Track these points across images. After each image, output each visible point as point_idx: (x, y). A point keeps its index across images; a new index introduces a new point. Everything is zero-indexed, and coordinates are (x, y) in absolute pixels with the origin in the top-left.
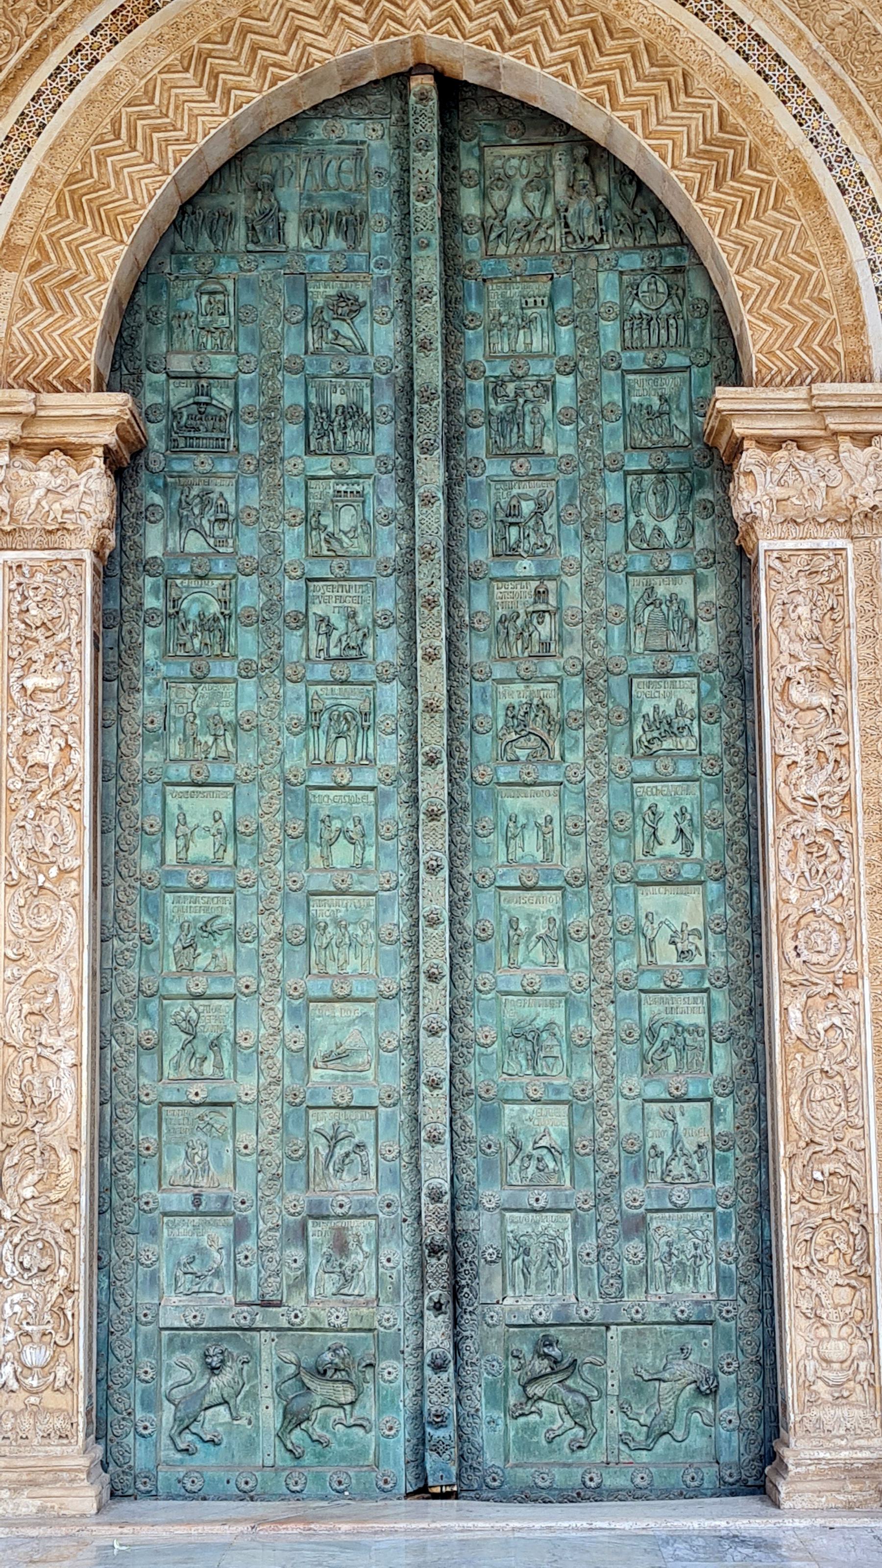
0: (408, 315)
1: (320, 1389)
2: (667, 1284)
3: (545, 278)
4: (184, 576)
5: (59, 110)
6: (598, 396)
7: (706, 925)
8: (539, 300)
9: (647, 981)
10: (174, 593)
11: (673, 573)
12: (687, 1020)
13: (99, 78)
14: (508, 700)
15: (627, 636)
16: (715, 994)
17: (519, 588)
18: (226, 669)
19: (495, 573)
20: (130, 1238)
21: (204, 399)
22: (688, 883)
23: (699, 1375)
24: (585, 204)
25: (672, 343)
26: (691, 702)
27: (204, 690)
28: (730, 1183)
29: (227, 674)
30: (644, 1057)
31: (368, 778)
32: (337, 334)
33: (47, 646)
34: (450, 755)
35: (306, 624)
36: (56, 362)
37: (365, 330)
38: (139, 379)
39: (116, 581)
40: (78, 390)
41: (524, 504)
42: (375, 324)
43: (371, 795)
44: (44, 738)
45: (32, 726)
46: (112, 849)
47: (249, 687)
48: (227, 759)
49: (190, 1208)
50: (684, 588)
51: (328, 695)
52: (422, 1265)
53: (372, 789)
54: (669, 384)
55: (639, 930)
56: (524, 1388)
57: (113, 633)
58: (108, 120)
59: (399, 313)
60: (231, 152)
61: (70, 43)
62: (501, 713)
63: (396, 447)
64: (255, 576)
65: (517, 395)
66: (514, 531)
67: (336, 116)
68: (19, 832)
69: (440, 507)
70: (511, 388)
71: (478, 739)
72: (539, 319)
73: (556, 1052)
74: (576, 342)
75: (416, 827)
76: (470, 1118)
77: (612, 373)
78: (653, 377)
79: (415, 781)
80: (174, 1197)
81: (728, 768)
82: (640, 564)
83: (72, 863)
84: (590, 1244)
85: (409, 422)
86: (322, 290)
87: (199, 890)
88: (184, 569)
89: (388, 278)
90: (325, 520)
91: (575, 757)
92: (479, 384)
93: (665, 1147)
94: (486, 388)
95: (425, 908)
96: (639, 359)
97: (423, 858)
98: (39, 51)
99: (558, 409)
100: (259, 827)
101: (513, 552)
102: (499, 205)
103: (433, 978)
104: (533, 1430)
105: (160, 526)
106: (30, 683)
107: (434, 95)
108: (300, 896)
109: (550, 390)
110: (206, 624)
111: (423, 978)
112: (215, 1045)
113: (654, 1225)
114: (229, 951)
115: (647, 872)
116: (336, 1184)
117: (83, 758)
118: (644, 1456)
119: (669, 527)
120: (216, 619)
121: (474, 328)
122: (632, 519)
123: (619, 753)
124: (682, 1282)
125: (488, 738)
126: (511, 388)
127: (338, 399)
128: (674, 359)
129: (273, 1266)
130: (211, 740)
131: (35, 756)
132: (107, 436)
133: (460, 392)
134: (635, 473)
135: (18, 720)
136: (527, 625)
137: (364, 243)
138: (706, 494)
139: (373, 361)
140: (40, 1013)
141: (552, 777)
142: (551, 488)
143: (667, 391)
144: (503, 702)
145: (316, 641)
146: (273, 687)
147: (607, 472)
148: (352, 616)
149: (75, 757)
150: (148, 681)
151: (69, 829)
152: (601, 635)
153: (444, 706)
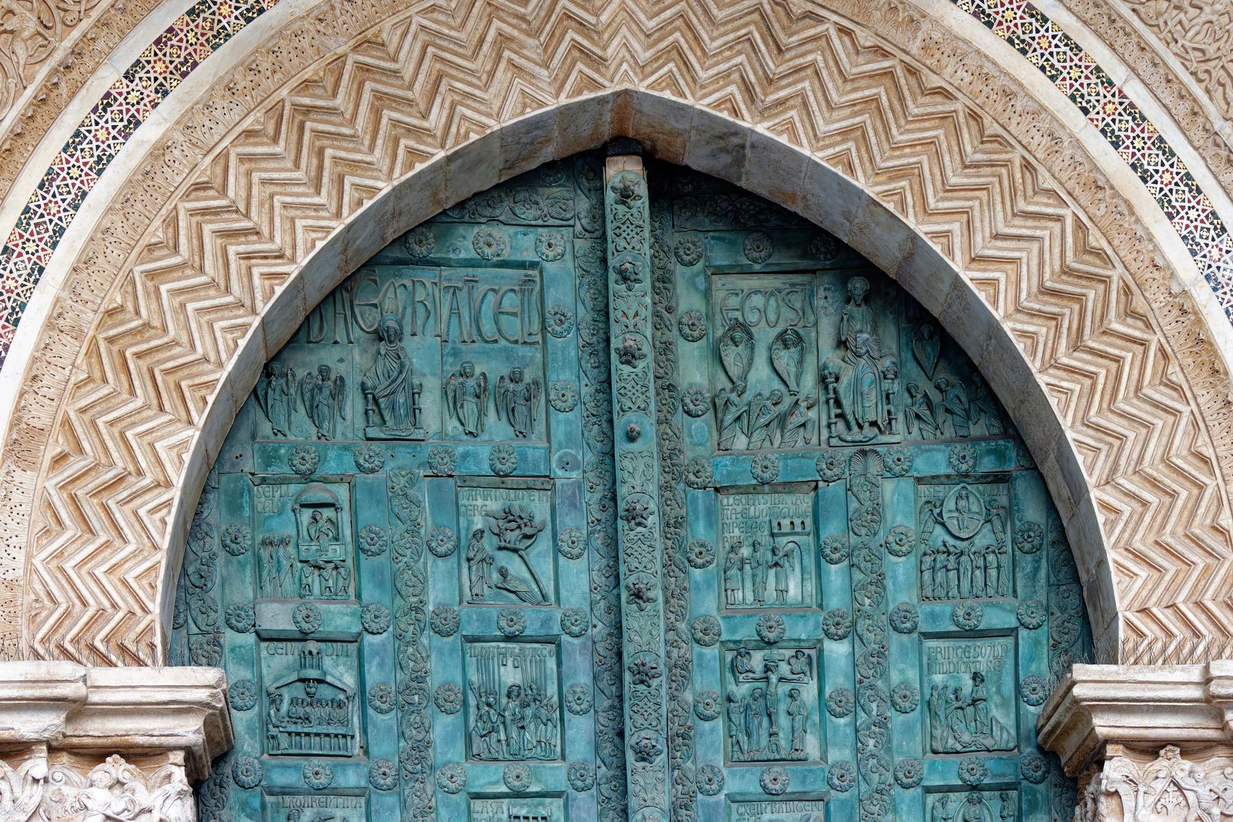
0: (613, 543)
3: (805, 487)
5: (84, 205)
6: (884, 675)
8: (797, 522)
13: (142, 152)
24: (865, 371)
25: (991, 591)
32: (503, 573)
37: (544, 568)
42: (562, 560)
54: (986, 654)
58: (157, 222)
59: (598, 540)
60: (340, 276)
65: (767, 669)
70: (757, 660)
72: (796, 554)
77: (905, 638)
78: (963, 643)
86: (479, 502)
94: (722, 659)
96: (944, 614)
99: (828, 691)
107: (642, 189)
109: (817, 665)
121: (703, 566)
126: (757, 660)
127: (510, 676)
134: (938, 789)
139: (558, 616)
143: (982, 668)
147: (899, 789)
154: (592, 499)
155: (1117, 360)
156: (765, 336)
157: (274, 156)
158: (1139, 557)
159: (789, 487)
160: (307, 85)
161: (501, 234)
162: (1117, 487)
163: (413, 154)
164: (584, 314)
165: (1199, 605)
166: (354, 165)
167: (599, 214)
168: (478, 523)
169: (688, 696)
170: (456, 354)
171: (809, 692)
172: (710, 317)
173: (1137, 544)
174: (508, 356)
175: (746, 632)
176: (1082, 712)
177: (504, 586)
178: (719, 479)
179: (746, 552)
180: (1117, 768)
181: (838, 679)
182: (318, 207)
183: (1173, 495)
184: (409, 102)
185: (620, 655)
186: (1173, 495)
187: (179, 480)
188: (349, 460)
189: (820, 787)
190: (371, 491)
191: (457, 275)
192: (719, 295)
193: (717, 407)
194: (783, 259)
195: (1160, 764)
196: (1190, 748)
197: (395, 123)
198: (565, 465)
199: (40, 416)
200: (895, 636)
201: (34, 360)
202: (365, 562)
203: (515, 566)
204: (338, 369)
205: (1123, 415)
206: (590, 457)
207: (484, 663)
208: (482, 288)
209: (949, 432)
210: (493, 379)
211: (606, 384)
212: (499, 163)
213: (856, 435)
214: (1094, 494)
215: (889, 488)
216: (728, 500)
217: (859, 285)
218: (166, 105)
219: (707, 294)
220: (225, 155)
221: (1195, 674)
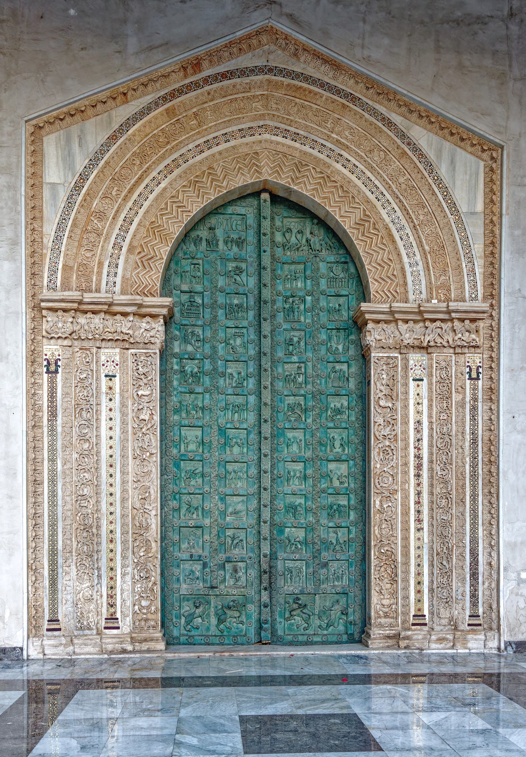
0: (260, 274)
1: (229, 613)
4: (186, 359)
7: (349, 474)
11: (342, 362)
13: (161, 189)
14: (288, 402)
15: (326, 382)
16: (351, 495)
17: (292, 366)
18: (200, 389)
19: (285, 361)
20: (171, 568)
21: (192, 300)
24: (316, 239)
26: (346, 404)
27: (193, 396)
29: (200, 391)
31: (245, 426)
32: (235, 280)
33: (145, 381)
35: (225, 376)
36: (146, 286)
37: (244, 279)
38: (171, 293)
39: (164, 360)
40: (154, 296)
41: (294, 338)
43: (245, 431)
44: (144, 411)
45: (141, 407)
47: (207, 396)
48: (200, 419)
49: (189, 559)
50: (345, 367)
51: (231, 399)
52: (261, 576)
53: (246, 429)
54: (342, 300)
59: (256, 273)
61: (151, 177)
62: (286, 406)
66: (291, 347)
68: (137, 441)
70: (291, 300)
71: (279, 414)
73: (302, 512)
79: (260, 427)
80: (184, 555)
81: (357, 425)
82: (331, 359)
83: (154, 451)
87: (191, 460)
88: (186, 356)
90: (232, 342)
91: (310, 421)
95: (263, 467)
96: (332, 291)
97: (263, 452)
98: (140, 179)
100: (211, 441)
101: (291, 354)
103: (265, 489)
105: (178, 342)
106: (140, 393)
107: (269, 200)
108: (223, 463)
109: (304, 301)
111: (262, 489)
112: (197, 509)
114: (201, 480)
115: (331, 457)
116: (234, 552)
117: (157, 418)
119: (340, 347)
120: (197, 373)
122: (329, 344)
123: (323, 420)
126: (291, 300)
127: (236, 302)
129: (215, 576)
130: (195, 412)
131: (142, 417)
135: (136, 405)
136: (295, 377)
138: (352, 337)
140: (145, 499)
141: (302, 426)
142: (303, 333)
143: (341, 303)
144: (287, 402)
146: (216, 396)
148: (239, 373)
149: (155, 417)
150: (175, 393)
151: (153, 441)
152: (318, 382)
154: (255, 264)
155: (372, 238)
156: (295, 231)
157: (189, 191)
158: (376, 280)
159: (299, 263)
160: (197, 176)
161: (237, 208)
162: (371, 265)
163: (219, 191)
164: (255, 226)
165: (389, 291)
166: (206, 193)
167: (259, 205)
169: (275, 307)
170: (227, 233)
171: (302, 307)
172: (283, 227)
173: (376, 278)
174: (238, 234)
176: (363, 313)
178: (284, 261)
179: (289, 277)
180: (370, 326)
181: (308, 305)
182: (198, 202)
183: (384, 267)
184: (219, 180)
185: (260, 298)
186: (384, 267)
187: (165, 258)
188: (202, 254)
189: (304, 328)
190: (207, 261)
191: (227, 217)
192: (285, 222)
193: (284, 246)
194: (300, 215)
195: (380, 325)
196: (386, 322)
197: (216, 185)
199: (135, 244)
200: (321, 296)
201: (135, 232)
202: (205, 276)
203: (238, 278)
204: (201, 236)
205: (373, 250)
206: (255, 256)
207: (230, 298)
208: (233, 219)
209: (334, 253)
210: (235, 238)
212: (238, 193)
213: (314, 252)
214: (366, 267)
215: (321, 264)
216: (285, 266)
217: (315, 221)
218: (166, 180)
219: (282, 222)
220: (179, 190)
221: (388, 305)
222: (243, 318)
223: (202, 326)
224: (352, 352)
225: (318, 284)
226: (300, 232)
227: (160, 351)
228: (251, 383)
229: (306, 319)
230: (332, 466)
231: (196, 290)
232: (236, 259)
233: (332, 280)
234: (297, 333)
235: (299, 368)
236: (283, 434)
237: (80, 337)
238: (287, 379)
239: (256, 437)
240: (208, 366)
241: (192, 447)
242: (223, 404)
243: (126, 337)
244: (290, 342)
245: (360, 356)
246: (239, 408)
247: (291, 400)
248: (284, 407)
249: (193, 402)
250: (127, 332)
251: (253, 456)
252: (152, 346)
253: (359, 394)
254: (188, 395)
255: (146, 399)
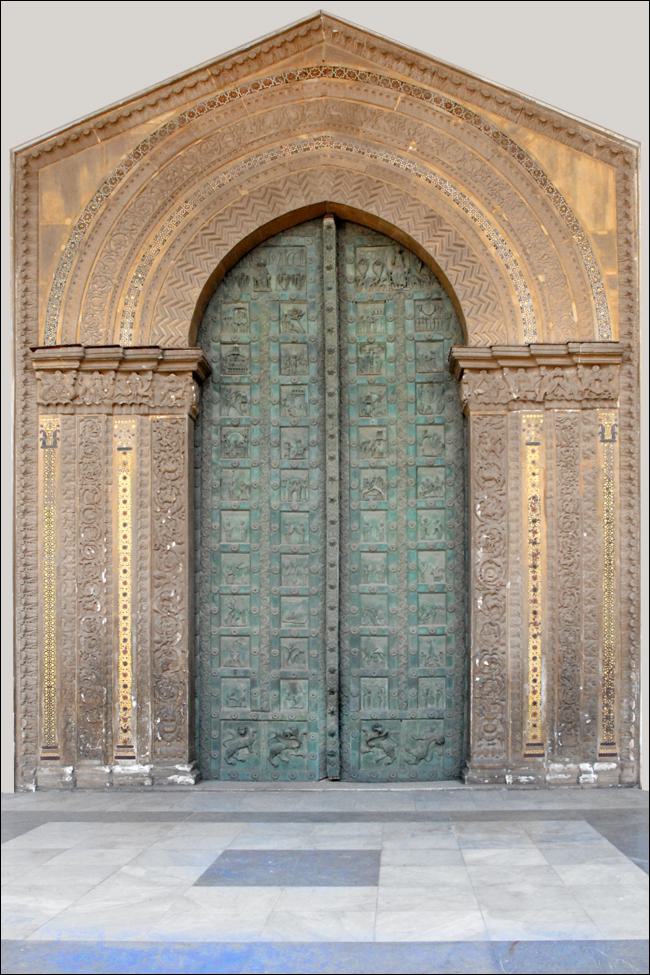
0: (323, 318)
2: (426, 704)
4: (228, 426)
6: (404, 351)
7: (446, 567)
9: (420, 590)
10: (224, 433)
12: (437, 604)
14: (366, 477)
15: (416, 451)
22: (439, 550)
23: (437, 737)
26: (442, 477)
27: (237, 472)
28: (452, 667)
29: (247, 465)
30: (419, 619)
31: (306, 508)
32: (293, 326)
34: (340, 498)
35: (279, 445)
38: (209, 345)
43: (307, 515)
46: (199, 536)
47: (256, 471)
55: (418, 569)
56: (367, 742)
57: (200, 448)
59: (320, 317)
63: (318, 372)
64: (258, 426)
66: (368, 406)
67: (292, 235)
69: (336, 398)
70: (367, 347)
74: (396, 329)
75: (325, 527)
76: (347, 642)
79: (325, 509)
81: (457, 504)
82: (422, 421)
84: (395, 690)
85: (323, 361)
88: (228, 423)
89: (314, 303)
90: (288, 403)
92: (354, 346)
93: (426, 653)
99: (388, 356)
100: (260, 528)
102: (363, 271)
104: (370, 758)
107: (334, 227)
109: (384, 349)
110: (237, 445)
113: (420, 683)
118: (414, 766)
119: (434, 406)
122: (419, 402)
124: (432, 703)
125: (357, 491)
127: (294, 353)
128: (436, 337)
130: (239, 492)
132: (194, 366)
133: (346, 350)
136: (373, 445)
137: (304, 288)
138: (449, 393)
141: (383, 507)
142: (384, 389)
143: (434, 349)
145: (284, 452)
150: (214, 467)
152: (404, 450)
153: (337, 478)
159: (377, 302)
161: (294, 238)
164: (317, 257)
167: (321, 233)
168: (286, 313)
175: (364, 340)
177: (293, 329)
181: (391, 353)
189: (384, 382)
198: (311, 297)
211: (322, 277)
222: (304, 373)
223: (248, 384)
224: (447, 413)
225: (404, 327)
226: (377, 263)
227: (190, 416)
228: (313, 456)
229: (387, 373)
230: (424, 556)
231: (240, 341)
232: (293, 301)
233: (418, 321)
234: (375, 389)
235: (380, 433)
236: (359, 516)
237: (84, 403)
238: (363, 447)
239: (321, 522)
240: (256, 434)
241: (236, 535)
242: (276, 481)
243: (145, 400)
244: (368, 401)
245: (461, 416)
246: (300, 486)
247: (368, 474)
248: (360, 484)
249: (237, 480)
250: (146, 394)
251: (316, 546)
252: (181, 411)
253: (459, 465)
254: (231, 471)
255: (173, 476)
